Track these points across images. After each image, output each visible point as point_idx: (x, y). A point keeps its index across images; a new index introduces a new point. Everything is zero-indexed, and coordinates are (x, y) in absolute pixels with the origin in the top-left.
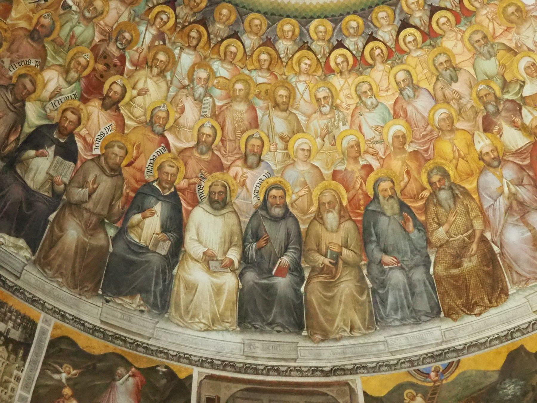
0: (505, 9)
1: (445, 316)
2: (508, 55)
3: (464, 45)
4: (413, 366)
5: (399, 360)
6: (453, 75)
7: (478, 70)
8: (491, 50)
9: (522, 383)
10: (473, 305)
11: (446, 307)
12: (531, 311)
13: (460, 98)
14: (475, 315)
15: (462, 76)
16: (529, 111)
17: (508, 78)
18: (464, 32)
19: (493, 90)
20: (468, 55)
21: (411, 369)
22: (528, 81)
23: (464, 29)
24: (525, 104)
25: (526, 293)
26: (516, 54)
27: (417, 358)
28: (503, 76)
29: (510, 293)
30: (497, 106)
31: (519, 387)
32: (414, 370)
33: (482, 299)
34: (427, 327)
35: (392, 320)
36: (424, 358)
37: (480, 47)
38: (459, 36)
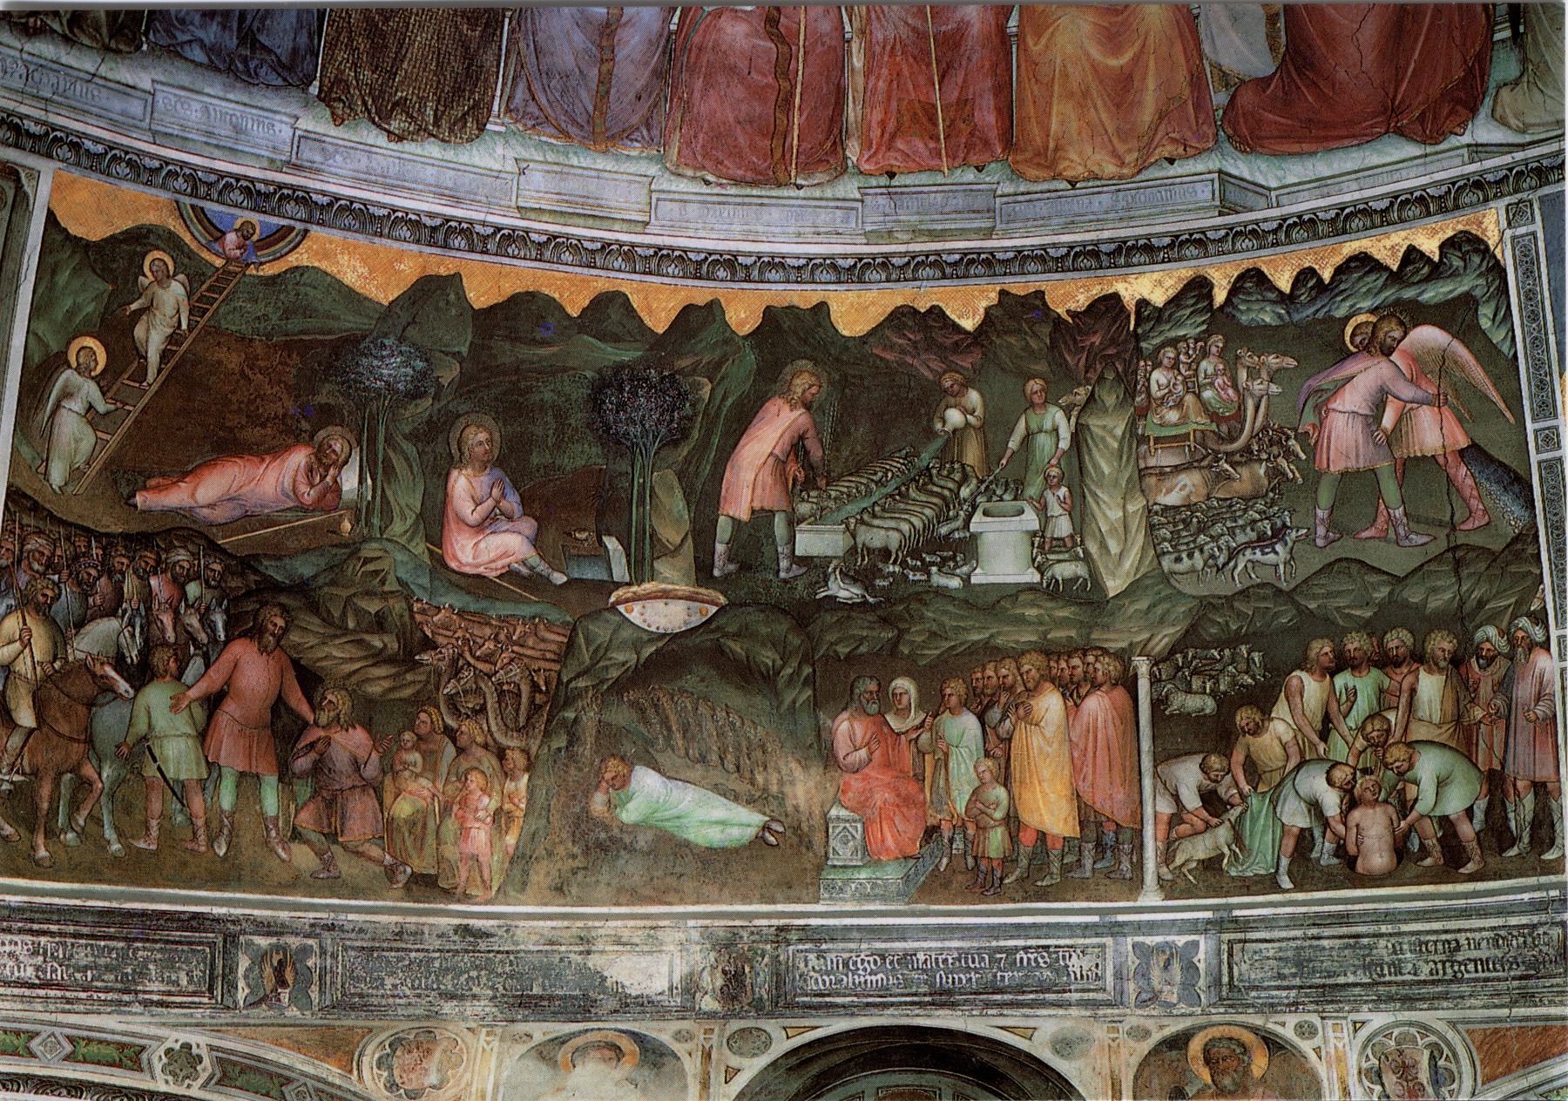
1: (318, 96)
4: (194, 194)
5: (167, 164)
9: (420, 364)
10: (396, 104)
11: (332, 73)
12: (513, 204)
14: (389, 132)
21: (187, 201)
25: (524, 154)
27: (213, 178)
29: (488, 126)
31: (409, 371)
32: (192, 206)
33: (423, 100)
34: (267, 105)
35: (186, 38)
36: (227, 185)
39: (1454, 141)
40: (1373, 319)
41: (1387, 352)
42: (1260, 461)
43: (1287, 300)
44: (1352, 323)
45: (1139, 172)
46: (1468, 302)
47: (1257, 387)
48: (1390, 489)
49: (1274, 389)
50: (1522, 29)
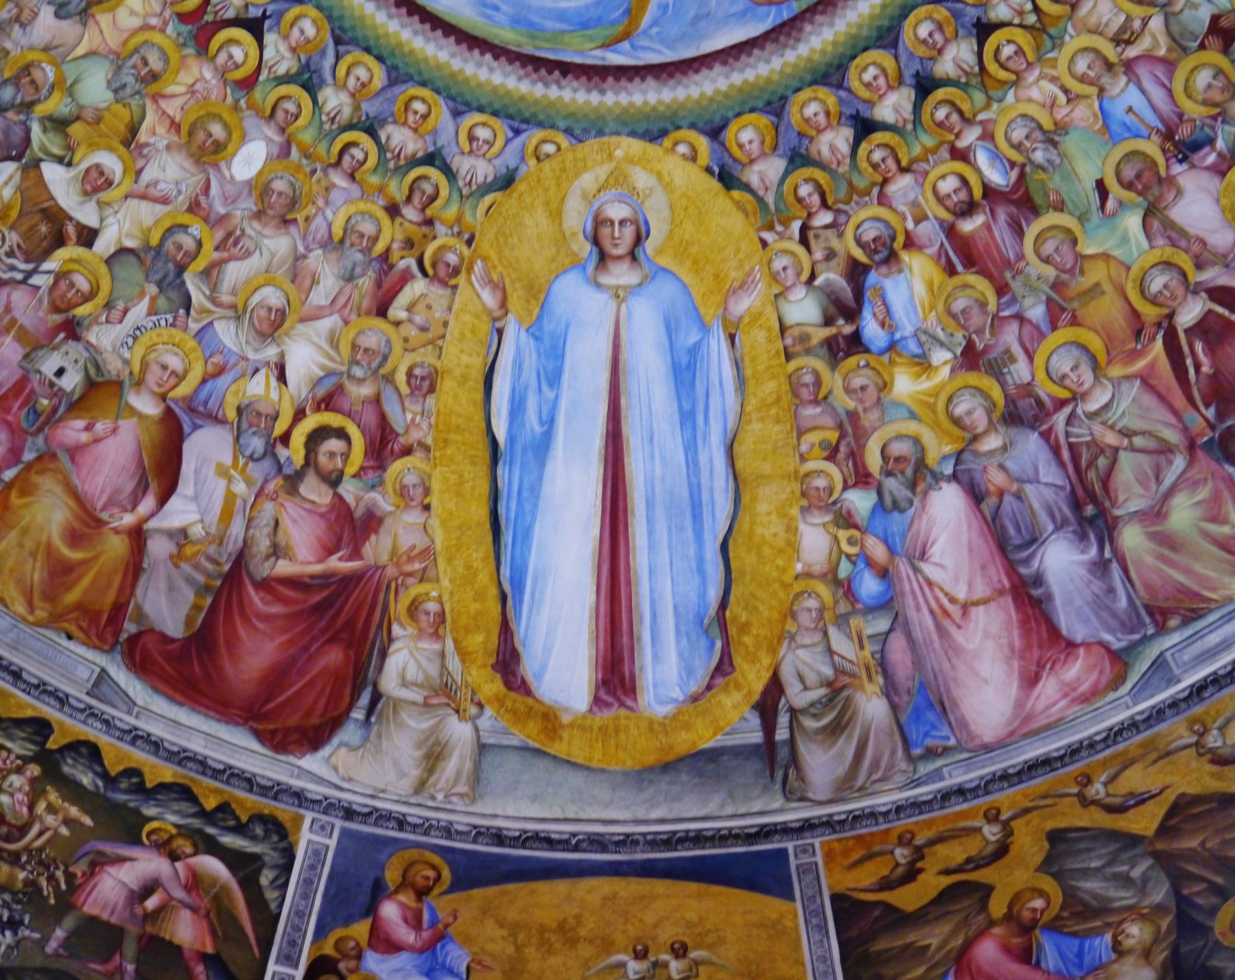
0: (217, 117)
2: (122, 128)
3: (135, 32)
6: (71, 8)
7: (86, 63)
8: (128, 91)
13: (23, 26)
15: (68, 29)
16: (11, 178)
17: (76, 130)
18: (163, 31)
19: (46, 98)
20: (113, 40)
22: (73, 172)
23: (169, 30)
24: (25, 169)
26: (127, 143)
28: (78, 118)
30: (13, 106)
37: (134, 67)
38: (154, 21)
39: (291, 759)
40: (174, 831)
41: (174, 857)
42: (23, 868)
43: (111, 781)
44: (154, 825)
45: (41, 626)
46: (255, 857)
47: (50, 820)
48: (130, 948)
49: (64, 831)
50: (373, 719)
